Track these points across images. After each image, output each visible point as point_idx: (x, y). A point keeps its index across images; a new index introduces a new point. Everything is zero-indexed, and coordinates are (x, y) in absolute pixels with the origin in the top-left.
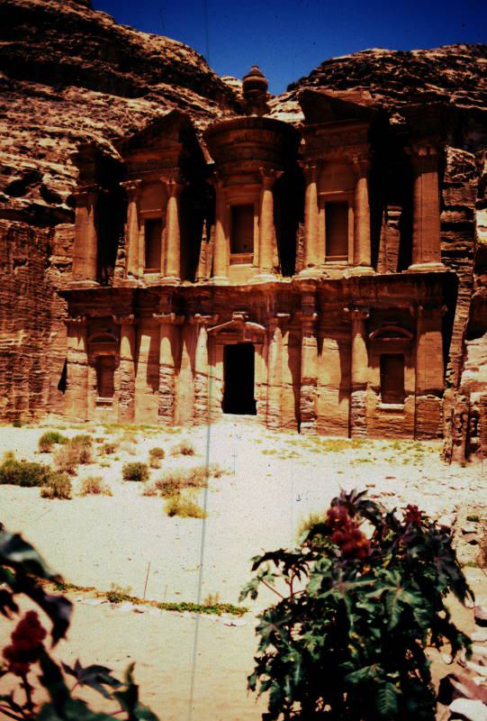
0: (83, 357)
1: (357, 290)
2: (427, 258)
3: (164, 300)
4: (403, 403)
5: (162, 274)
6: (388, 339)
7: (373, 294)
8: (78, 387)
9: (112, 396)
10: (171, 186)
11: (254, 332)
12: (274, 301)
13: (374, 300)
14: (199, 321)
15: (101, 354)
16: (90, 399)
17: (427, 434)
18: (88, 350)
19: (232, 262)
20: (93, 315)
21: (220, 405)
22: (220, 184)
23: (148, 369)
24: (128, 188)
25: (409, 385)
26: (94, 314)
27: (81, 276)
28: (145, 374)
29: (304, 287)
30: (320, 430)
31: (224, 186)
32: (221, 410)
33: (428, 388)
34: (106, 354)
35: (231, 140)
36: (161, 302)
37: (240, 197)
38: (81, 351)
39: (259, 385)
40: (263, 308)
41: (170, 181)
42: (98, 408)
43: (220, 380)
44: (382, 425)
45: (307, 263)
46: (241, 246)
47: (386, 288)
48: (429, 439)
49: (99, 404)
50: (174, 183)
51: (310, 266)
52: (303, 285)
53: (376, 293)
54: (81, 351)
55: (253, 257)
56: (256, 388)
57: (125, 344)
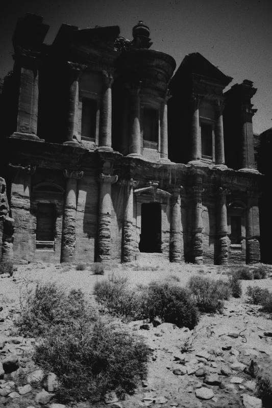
0: (26, 203)
1: (224, 177)
2: (250, 166)
3: (107, 164)
4: (241, 244)
5: (97, 143)
6: (235, 208)
7: (230, 182)
8: (24, 231)
9: (53, 240)
10: (110, 79)
11: (161, 195)
12: (176, 177)
13: (231, 185)
14: (131, 184)
15: (42, 201)
16: (30, 241)
17: (255, 260)
18: (32, 198)
19: (144, 145)
20: (41, 166)
21: (138, 246)
22: (139, 90)
23: (85, 217)
24: (74, 68)
25: (244, 234)
26: (42, 165)
27: (27, 129)
28: (82, 222)
29: (199, 171)
30: (204, 263)
31: (140, 93)
32: (138, 249)
33: (255, 235)
34: (48, 202)
35: (154, 64)
36: (104, 165)
37: (153, 104)
38: (26, 197)
39: (165, 232)
40: (167, 180)
41: (109, 76)
42: (38, 251)
43: (139, 228)
44: (233, 256)
45: (197, 157)
46: (151, 137)
47: (236, 179)
48: (256, 263)
49: (38, 247)
50: (111, 77)
51: (198, 159)
52: (198, 170)
53: (232, 181)
54: (26, 197)
55: (158, 146)
56: (163, 234)
57: (72, 194)
